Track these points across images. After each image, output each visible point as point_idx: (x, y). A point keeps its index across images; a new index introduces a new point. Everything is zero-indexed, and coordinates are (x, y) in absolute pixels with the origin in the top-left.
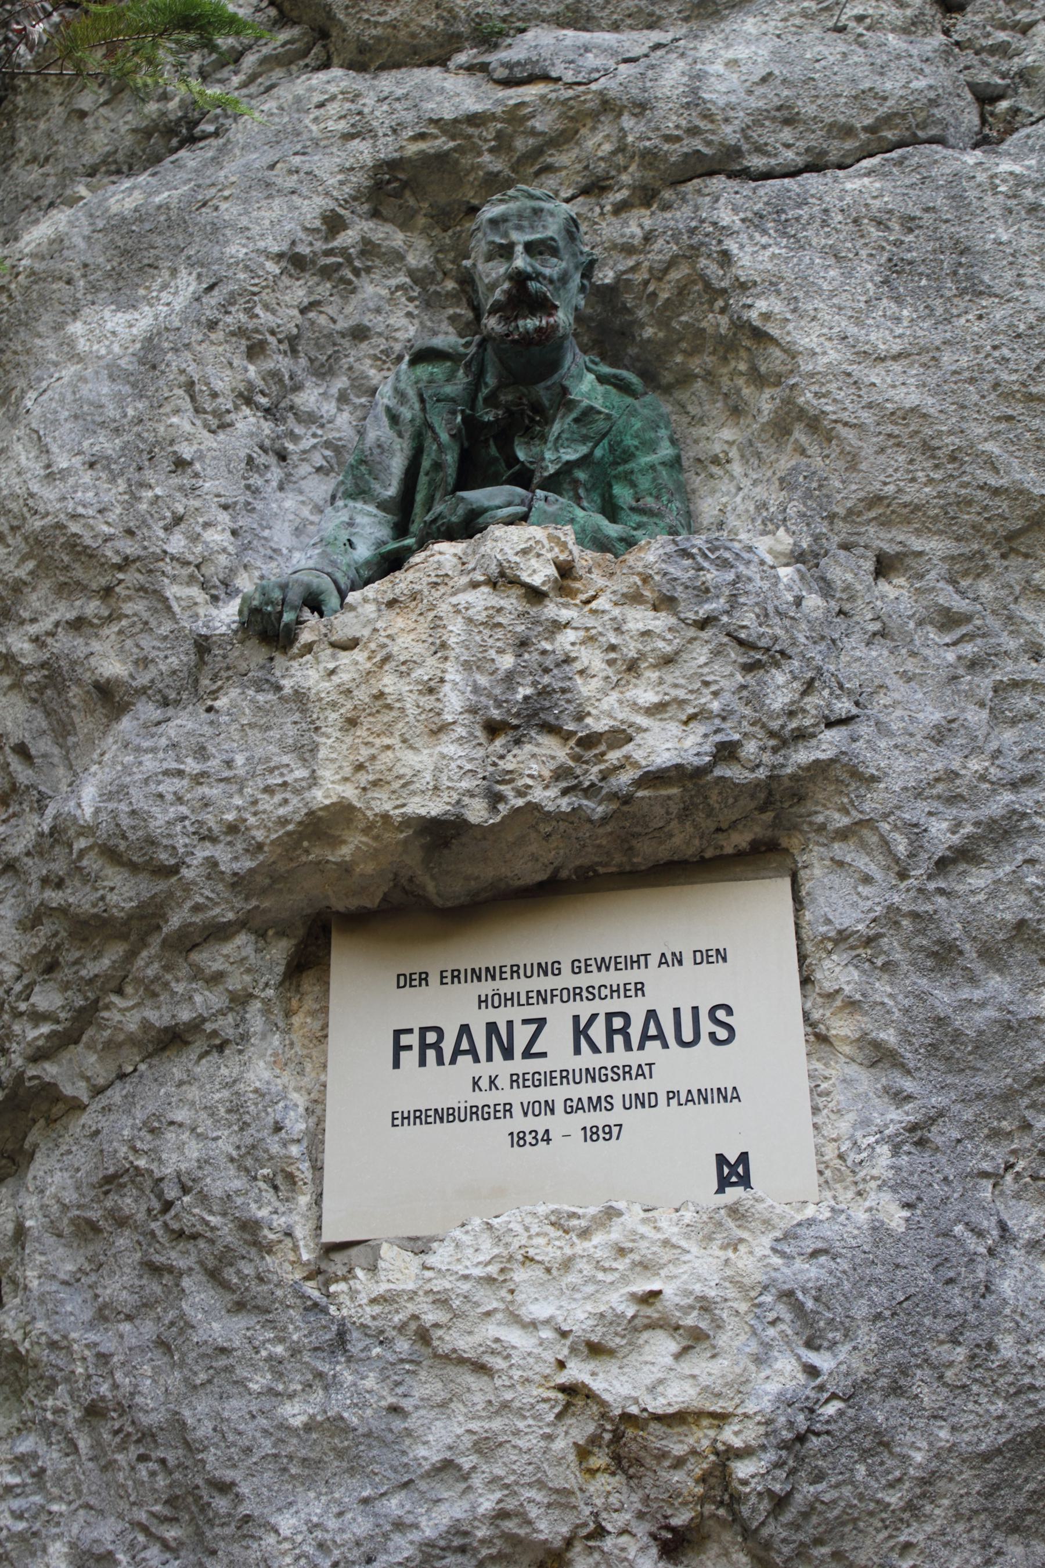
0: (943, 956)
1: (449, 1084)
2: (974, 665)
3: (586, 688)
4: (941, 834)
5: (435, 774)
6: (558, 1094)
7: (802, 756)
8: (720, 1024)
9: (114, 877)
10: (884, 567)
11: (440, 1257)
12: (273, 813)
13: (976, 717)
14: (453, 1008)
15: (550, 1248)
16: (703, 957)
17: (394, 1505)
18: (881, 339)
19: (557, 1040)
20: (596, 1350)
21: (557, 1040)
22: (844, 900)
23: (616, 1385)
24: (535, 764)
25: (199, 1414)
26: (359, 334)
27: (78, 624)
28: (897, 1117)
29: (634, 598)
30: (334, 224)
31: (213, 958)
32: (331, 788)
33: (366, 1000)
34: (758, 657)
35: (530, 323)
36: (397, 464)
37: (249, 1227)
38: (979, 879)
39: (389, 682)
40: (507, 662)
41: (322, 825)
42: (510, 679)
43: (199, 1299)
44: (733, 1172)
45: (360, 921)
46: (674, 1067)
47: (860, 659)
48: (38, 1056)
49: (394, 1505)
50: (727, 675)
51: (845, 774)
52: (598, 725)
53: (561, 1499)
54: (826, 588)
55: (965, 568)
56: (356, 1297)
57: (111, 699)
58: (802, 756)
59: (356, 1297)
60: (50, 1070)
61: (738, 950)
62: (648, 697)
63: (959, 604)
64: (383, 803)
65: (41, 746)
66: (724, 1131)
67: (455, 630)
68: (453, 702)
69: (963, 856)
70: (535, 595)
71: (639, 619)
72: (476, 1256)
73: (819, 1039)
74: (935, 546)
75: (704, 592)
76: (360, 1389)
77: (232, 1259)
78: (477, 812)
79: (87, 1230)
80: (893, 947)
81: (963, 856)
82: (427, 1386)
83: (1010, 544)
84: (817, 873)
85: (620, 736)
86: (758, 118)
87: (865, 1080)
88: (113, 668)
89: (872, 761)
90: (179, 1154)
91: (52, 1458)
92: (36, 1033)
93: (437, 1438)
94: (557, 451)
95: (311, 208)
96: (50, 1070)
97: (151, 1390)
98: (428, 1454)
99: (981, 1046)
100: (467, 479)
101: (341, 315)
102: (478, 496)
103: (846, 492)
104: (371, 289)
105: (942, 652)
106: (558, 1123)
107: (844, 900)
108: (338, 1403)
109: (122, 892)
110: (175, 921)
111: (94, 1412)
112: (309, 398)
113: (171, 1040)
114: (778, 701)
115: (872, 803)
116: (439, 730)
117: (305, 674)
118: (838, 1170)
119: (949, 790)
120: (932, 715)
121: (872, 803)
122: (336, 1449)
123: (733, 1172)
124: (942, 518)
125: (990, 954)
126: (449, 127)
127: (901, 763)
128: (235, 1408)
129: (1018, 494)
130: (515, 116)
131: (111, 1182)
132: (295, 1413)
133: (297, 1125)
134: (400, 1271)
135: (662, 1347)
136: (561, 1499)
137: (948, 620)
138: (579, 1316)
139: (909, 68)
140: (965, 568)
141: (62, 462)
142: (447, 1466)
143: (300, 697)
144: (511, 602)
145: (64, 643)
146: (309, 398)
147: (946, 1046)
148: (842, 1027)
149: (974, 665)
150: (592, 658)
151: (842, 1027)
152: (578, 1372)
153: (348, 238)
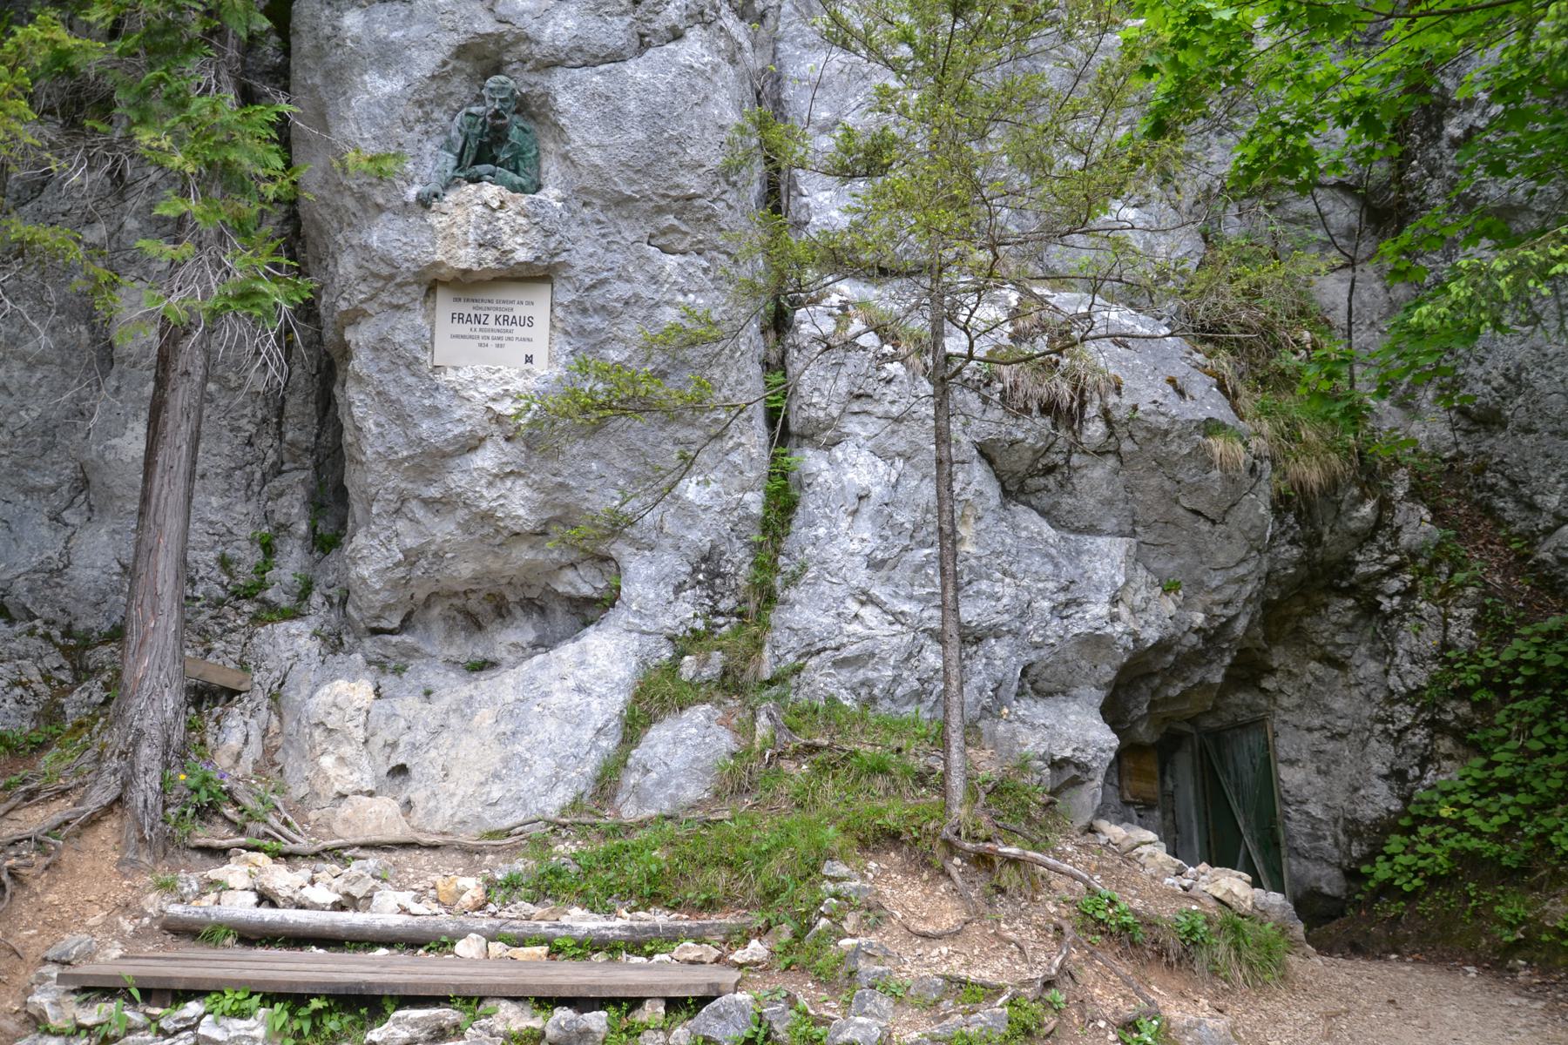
0: (584, 311)
1: (464, 329)
2: (604, 236)
3: (505, 237)
4: (588, 281)
5: (466, 258)
6: (490, 334)
7: (557, 259)
8: (529, 322)
9: (382, 265)
10: (585, 204)
11: (461, 373)
12: (425, 259)
13: (601, 251)
14: (467, 309)
15: (486, 376)
16: (528, 303)
17: (449, 426)
18: (594, 140)
19: (491, 320)
20: (494, 400)
21: (491, 320)
22: (566, 296)
23: (497, 407)
24: (490, 256)
25: (404, 398)
26: (451, 94)
27: (370, 184)
28: (569, 348)
29: (518, 213)
30: (445, 64)
31: (408, 290)
32: (439, 257)
33: (445, 305)
34: (548, 234)
35: (499, 122)
36: (460, 143)
37: (417, 359)
38: (596, 293)
39: (454, 230)
40: (485, 228)
41: (437, 265)
42: (486, 233)
43: (403, 371)
44: (529, 359)
45: (445, 284)
46: (518, 331)
47: (575, 231)
48: (361, 302)
49: (449, 426)
50: (539, 238)
51: (567, 265)
52: (507, 248)
53: (484, 429)
54: (569, 210)
55: (604, 209)
56: (441, 379)
57: (380, 209)
58: (557, 259)
59: (441, 379)
60: (364, 306)
61: (537, 306)
62: (520, 241)
63: (602, 218)
64: (452, 263)
65: (359, 214)
66: (528, 349)
67: (473, 218)
68: (471, 238)
69: (594, 287)
70: (494, 210)
71: (521, 220)
72: (469, 376)
73: (553, 327)
74: (597, 202)
75: (536, 215)
76: (442, 400)
77: (412, 364)
78: (475, 267)
79: (375, 349)
80: (572, 308)
81: (594, 287)
82: (456, 402)
83: (617, 204)
84: (557, 286)
85: (512, 251)
86: (571, 50)
87: (563, 338)
88: (381, 201)
89: (573, 262)
90: (399, 338)
91: (368, 401)
92: (362, 296)
93: (458, 414)
94: (504, 155)
95: (439, 57)
96: (364, 306)
97: (394, 391)
98: (457, 416)
99: (590, 333)
100: (476, 162)
101: (444, 90)
102: (480, 168)
103: (578, 184)
104: (456, 80)
105: (595, 231)
106: (490, 342)
107: (566, 296)
108: (437, 402)
109: (385, 270)
110: (398, 280)
111: (379, 393)
112: (435, 115)
113: (398, 307)
114: (552, 246)
115: (572, 273)
116: (467, 245)
117: (433, 219)
118: (552, 359)
119: (590, 270)
120: (591, 250)
121: (572, 273)
122: (434, 412)
123: (529, 359)
124: (602, 195)
125: (595, 310)
126: (481, 36)
127: (581, 262)
128: (413, 399)
129: (620, 192)
130: (501, 35)
131: (382, 340)
132: (427, 402)
133: (428, 335)
134: (451, 375)
135: (508, 401)
136: (484, 429)
137: (599, 222)
138: (491, 393)
139: (617, 30)
140: (604, 209)
141: (366, 136)
142: (460, 420)
143: (431, 227)
144: (487, 211)
145: (366, 189)
146: (435, 115)
147: (582, 332)
148: (559, 325)
149: (604, 236)
150: (507, 229)
151: (559, 325)
152: (490, 404)
153: (449, 67)
